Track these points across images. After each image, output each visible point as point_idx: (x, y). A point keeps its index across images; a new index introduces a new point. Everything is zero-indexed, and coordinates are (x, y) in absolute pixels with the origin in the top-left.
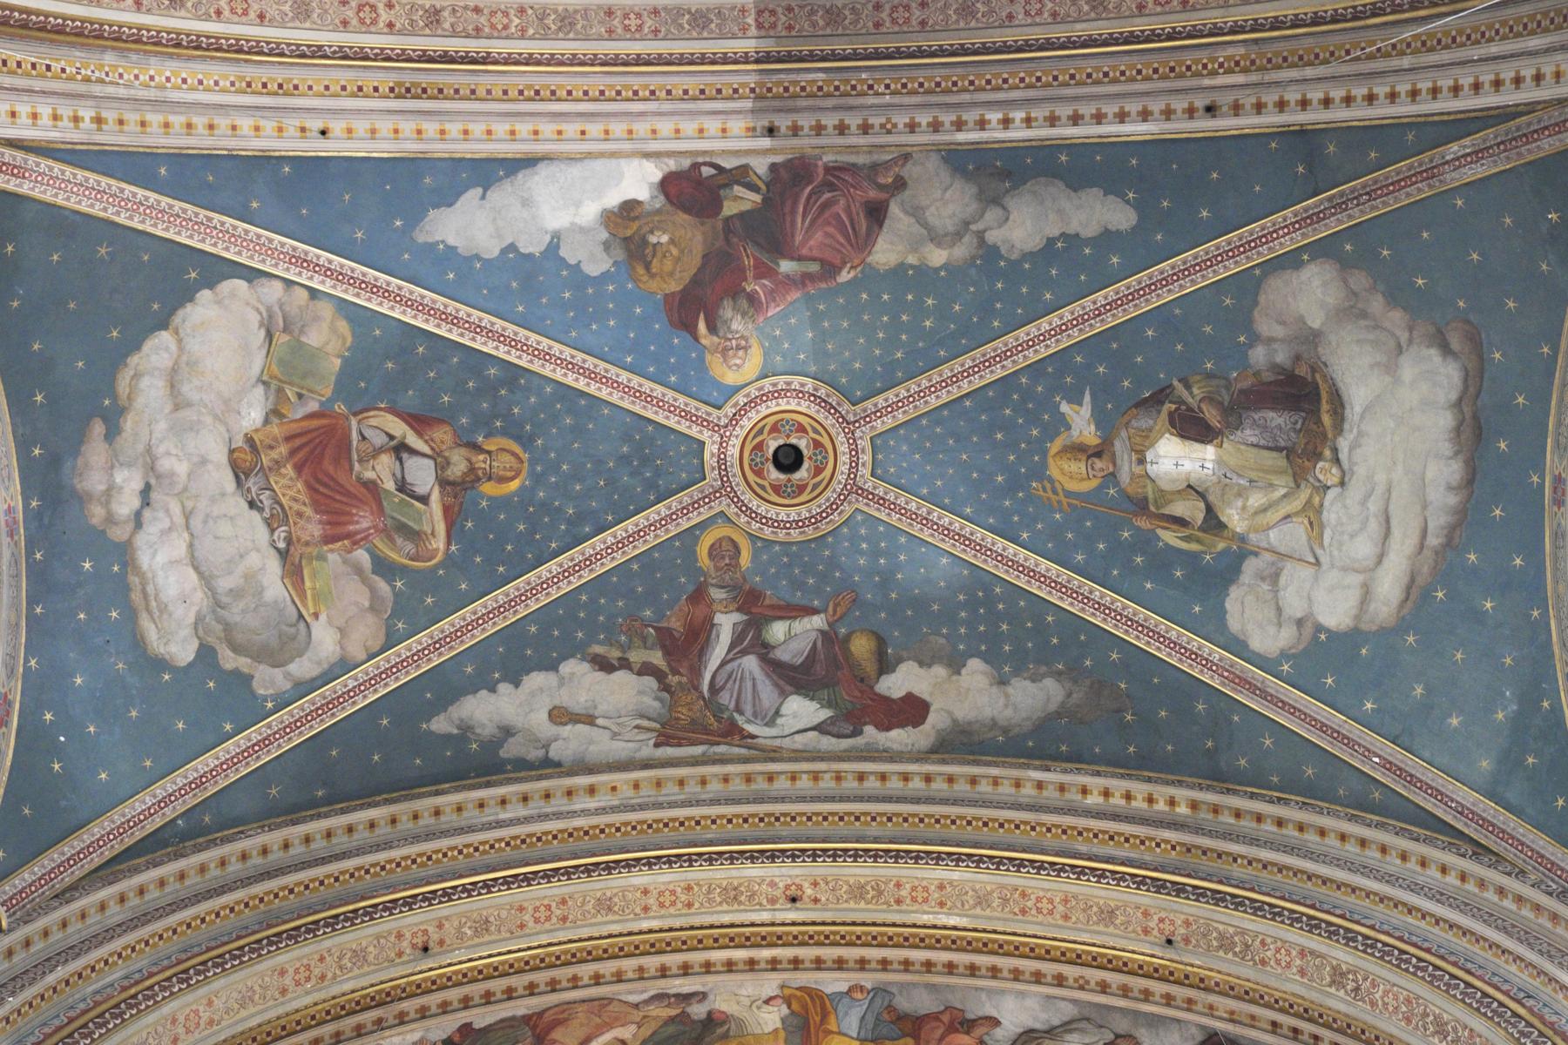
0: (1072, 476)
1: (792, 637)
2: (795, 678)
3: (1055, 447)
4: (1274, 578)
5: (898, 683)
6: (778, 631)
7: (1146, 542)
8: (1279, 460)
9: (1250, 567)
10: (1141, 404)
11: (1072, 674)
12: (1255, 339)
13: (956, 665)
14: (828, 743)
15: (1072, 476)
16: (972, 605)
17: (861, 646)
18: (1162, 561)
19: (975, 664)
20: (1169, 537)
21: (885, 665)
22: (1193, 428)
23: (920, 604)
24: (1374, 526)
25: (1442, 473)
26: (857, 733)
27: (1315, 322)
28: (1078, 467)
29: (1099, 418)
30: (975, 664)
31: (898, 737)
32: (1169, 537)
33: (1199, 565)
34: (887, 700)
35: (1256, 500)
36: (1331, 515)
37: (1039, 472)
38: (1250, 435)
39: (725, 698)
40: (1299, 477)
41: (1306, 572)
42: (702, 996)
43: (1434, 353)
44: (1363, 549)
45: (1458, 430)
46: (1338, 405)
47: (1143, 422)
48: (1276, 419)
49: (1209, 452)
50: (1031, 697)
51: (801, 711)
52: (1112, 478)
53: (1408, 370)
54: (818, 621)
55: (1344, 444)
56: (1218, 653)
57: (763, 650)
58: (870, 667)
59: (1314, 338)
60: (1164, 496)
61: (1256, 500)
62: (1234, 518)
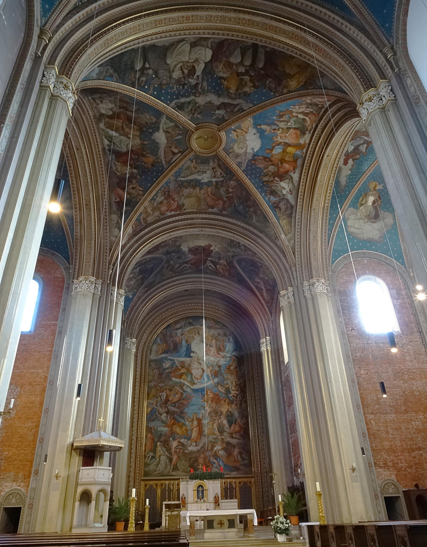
0: (372, 186)
1: (363, 148)
2: (357, 148)
3: (377, 183)
4: (354, 214)
5: (350, 162)
6: (365, 146)
7: (361, 195)
8: (368, 214)
9: (355, 210)
10: (379, 196)
11: (346, 186)
12: (385, 212)
13: (351, 170)
14: (345, 151)
15: (372, 186)
16: (359, 172)
17: (358, 157)
18: (358, 198)
19: (350, 172)
20: (361, 199)
21: (353, 160)
22: (374, 203)
23: (361, 165)
24: (359, 227)
25: (365, 236)
26: (345, 155)
27: (385, 220)
28: (373, 186)
29: (380, 189)
30: (350, 172)
31: (342, 161)
32: (361, 199)
33: (357, 204)
34: (348, 160)
35: (364, 211)
36: (361, 221)
37: (374, 181)
38: (372, 210)
39: (358, 139)
40: (366, 216)
41: (354, 218)
42: (309, 133)
43: (379, 236)
44: (356, 226)
45: (370, 238)
46: (374, 222)
47: (377, 195)
48: (374, 214)
49: (371, 204)
50: (343, 180)
51: (351, 148)
52: (371, 191)
53: (378, 232)
54: (364, 151)
55: (369, 223)
56: (346, 208)
57: (363, 144)
58: (354, 158)
59: (383, 220)
60: (366, 198)
61: (364, 211)
62: (362, 207)
